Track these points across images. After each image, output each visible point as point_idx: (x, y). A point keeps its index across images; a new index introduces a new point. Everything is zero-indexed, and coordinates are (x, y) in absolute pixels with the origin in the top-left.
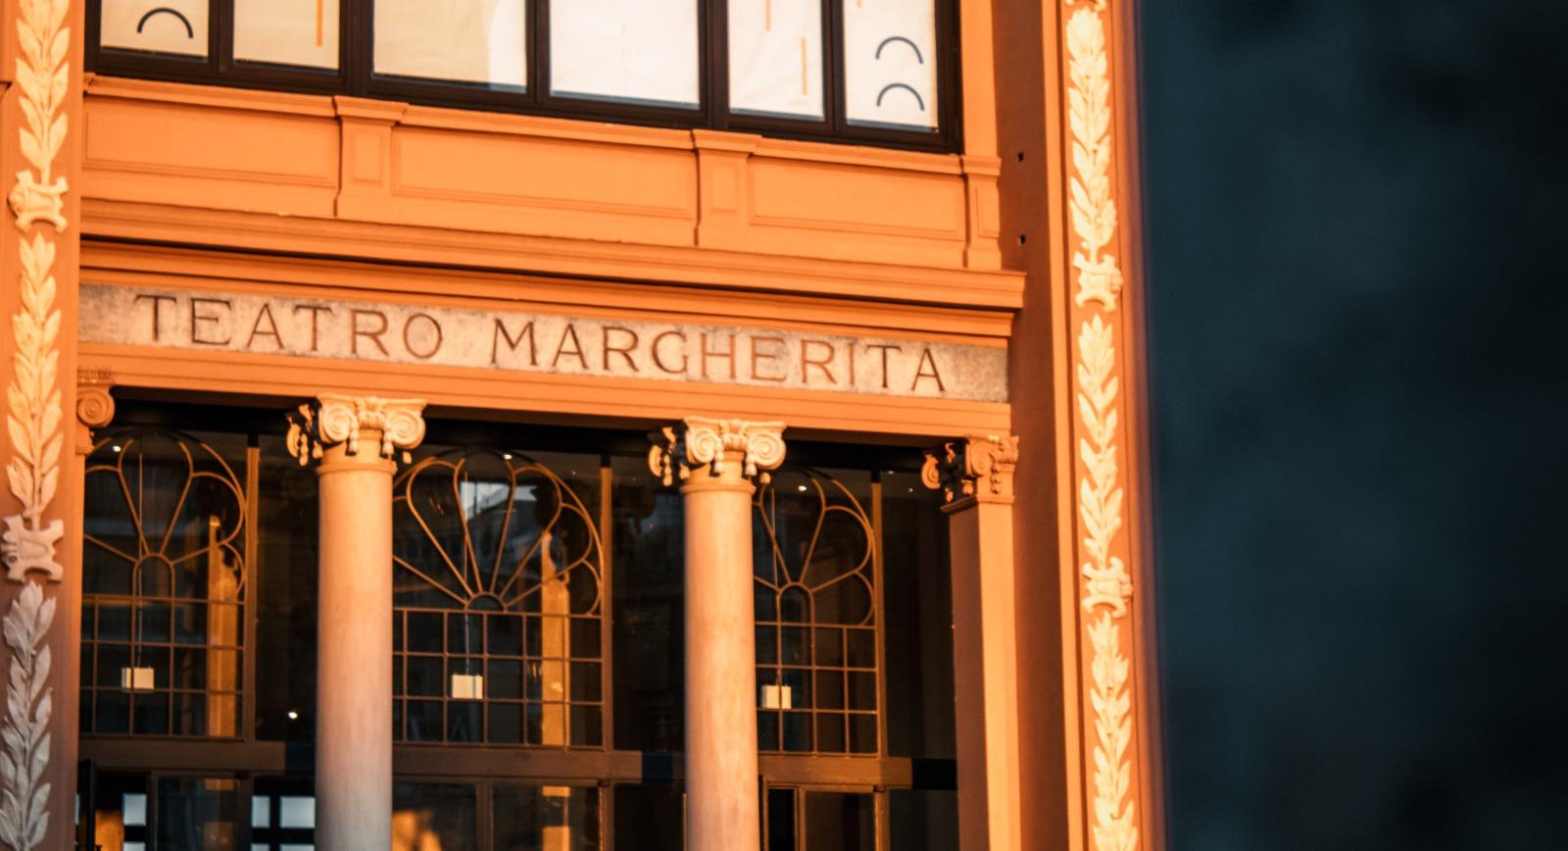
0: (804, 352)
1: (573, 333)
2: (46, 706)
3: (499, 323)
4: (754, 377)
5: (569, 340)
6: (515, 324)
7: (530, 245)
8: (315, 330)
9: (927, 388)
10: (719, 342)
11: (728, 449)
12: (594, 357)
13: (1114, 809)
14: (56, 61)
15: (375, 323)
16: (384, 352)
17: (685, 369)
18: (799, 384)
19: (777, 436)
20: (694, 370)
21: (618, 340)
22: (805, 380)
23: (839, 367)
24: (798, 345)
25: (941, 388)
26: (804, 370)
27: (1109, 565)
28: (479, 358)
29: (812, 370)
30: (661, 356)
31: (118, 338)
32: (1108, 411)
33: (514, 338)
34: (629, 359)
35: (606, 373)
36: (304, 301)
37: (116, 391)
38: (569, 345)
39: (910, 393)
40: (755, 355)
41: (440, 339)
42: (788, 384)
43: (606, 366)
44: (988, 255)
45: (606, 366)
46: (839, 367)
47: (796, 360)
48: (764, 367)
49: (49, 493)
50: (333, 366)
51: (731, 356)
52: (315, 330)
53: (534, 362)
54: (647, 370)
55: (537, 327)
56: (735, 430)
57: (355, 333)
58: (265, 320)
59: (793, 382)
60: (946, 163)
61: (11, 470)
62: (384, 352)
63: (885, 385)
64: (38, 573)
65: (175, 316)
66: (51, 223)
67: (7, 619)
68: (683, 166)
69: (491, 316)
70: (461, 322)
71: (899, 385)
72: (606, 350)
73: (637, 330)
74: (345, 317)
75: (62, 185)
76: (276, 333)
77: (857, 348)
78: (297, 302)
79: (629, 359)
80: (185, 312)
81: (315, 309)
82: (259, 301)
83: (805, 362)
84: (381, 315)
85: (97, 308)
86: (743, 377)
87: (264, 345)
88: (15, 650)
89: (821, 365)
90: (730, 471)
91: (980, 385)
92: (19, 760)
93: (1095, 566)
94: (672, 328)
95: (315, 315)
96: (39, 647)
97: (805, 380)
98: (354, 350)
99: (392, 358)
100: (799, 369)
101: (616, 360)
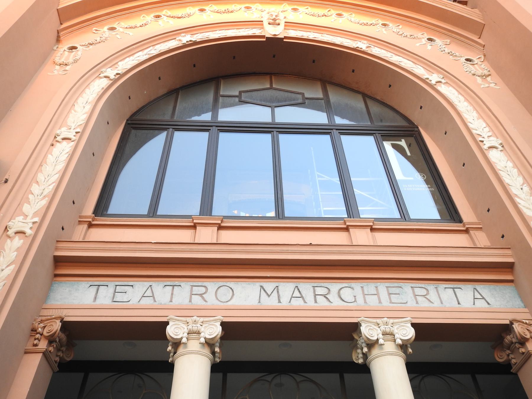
4: (391, 302)
6: (269, 286)
8: (172, 294)
10: (370, 287)
11: (385, 334)
14: (50, 182)
15: (203, 290)
16: (206, 301)
17: (355, 301)
18: (415, 304)
20: (360, 300)
21: (319, 291)
22: (417, 303)
23: (433, 295)
25: (488, 304)
34: (327, 298)
35: (316, 304)
36: (168, 283)
38: (297, 294)
41: (233, 294)
42: (409, 304)
43: (316, 302)
45: (316, 302)
46: (433, 295)
47: (412, 295)
48: (394, 298)
51: (377, 294)
52: (172, 294)
53: (280, 302)
55: (280, 288)
56: (387, 324)
59: (411, 304)
62: (206, 301)
63: (459, 304)
68: (344, 234)
72: (315, 295)
76: (153, 296)
77: (439, 289)
78: (165, 284)
79: (327, 298)
80: (111, 290)
82: (147, 284)
83: (415, 296)
85: (70, 291)
86: (386, 303)
90: (389, 347)
97: (417, 303)
98: (190, 301)
101: (320, 299)
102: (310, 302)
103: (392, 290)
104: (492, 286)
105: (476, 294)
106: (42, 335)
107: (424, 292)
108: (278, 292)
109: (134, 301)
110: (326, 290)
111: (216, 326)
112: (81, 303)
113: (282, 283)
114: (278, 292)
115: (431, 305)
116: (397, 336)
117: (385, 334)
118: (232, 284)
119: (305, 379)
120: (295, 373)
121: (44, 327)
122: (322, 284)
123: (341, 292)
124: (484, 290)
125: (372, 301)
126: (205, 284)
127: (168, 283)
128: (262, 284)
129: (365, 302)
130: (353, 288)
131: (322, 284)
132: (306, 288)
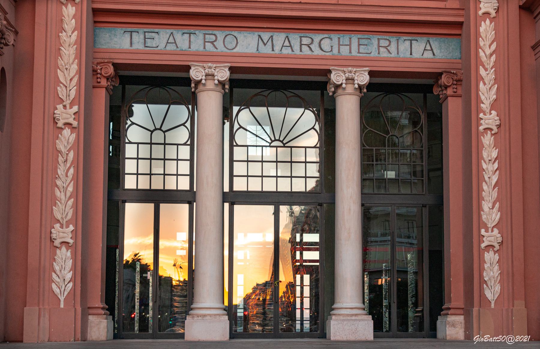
0: (379, 43)
1: (288, 39)
2: (72, 171)
3: (260, 36)
4: (359, 53)
5: (287, 41)
6: (266, 36)
7: (266, 5)
8: (190, 41)
10: (345, 39)
12: (296, 48)
13: (490, 205)
15: (213, 38)
16: (217, 48)
17: (331, 51)
18: (377, 55)
19: (367, 74)
20: (335, 51)
21: (305, 41)
22: (379, 53)
24: (377, 41)
25: (434, 55)
26: (379, 49)
27: (491, 114)
29: (382, 49)
30: (322, 46)
31: (117, 47)
32: (491, 55)
33: (265, 42)
34: (310, 47)
35: (301, 53)
36: (186, 31)
37: (114, 64)
38: (287, 43)
39: (421, 57)
40: (359, 45)
41: (237, 43)
42: (372, 55)
43: (301, 51)
45: (301, 51)
47: (376, 46)
49: (72, 96)
50: (197, 54)
51: (350, 45)
52: (190, 41)
53: (273, 50)
54: (317, 52)
55: (274, 37)
56: (350, 72)
57: (205, 42)
58: (171, 38)
59: (374, 54)
61: (59, 88)
62: (217, 48)
63: (411, 54)
64: (68, 124)
67: (57, 141)
69: (257, 34)
70: (245, 36)
71: (417, 55)
72: (301, 45)
73: (313, 37)
74: (201, 36)
76: (175, 43)
77: (400, 41)
78: (183, 32)
79: (310, 47)
80: (142, 36)
81: (190, 34)
82: (169, 31)
83: (379, 46)
84: (215, 35)
85: (110, 36)
86: (354, 53)
87: (171, 47)
88: (60, 152)
89: (386, 47)
91: (450, 53)
92: (62, 190)
93: (485, 114)
94: (327, 36)
95: (190, 36)
96: (69, 151)
97: (379, 53)
98: (204, 48)
99: (219, 50)
100: (377, 50)
101: (305, 48)
102: (297, 51)
103: (362, 42)
104: (443, 39)
105: (428, 45)
106: (101, 74)
107: (387, 43)
108: (272, 41)
109: (162, 46)
110: (310, 40)
111: (225, 71)
112: (121, 48)
113: (276, 33)
114: (272, 41)
115: (389, 55)
116: (356, 82)
119: (293, 95)
120: (285, 90)
121: (101, 69)
122: (308, 35)
123: (322, 42)
124: (435, 43)
125: (345, 51)
126: (215, 32)
127: (186, 31)
128: (260, 33)
129: (339, 52)
130: (331, 39)
131: (308, 35)
132: (295, 38)
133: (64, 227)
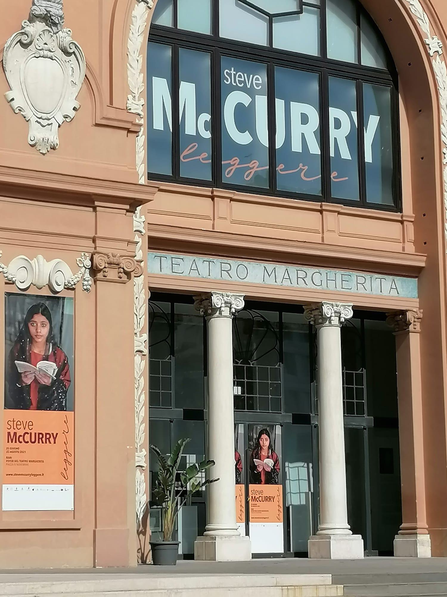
4: (342, 288)
9: (394, 293)
11: (335, 312)
12: (294, 280)
21: (301, 274)
23: (367, 285)
25: (398, 293)
28: (258, 280)
38: (286, 276)
39: (389, 295)
40: (342, 280)
44: (410, 248)
53: (276, 282)
54: (310, 285)
59: (354, 290)
60: (396, 216)
63: (381, 292)
65: (167, 263)
66: (141, 232)
70: (253, 267)
71: (385, 293)
75: (143, 218)
76: (197, 270)
81: (209, 262)
84: (229, 264)
86: (339, 288)
87: (194, 274)
91: (409, 292)
96: (140, 377)
99: (233, 279)
102: (295, 284)
109: (186, 273)
112: (153, 272)
117: (335, 312)
118: (246, 263)
133: (138, 451)
